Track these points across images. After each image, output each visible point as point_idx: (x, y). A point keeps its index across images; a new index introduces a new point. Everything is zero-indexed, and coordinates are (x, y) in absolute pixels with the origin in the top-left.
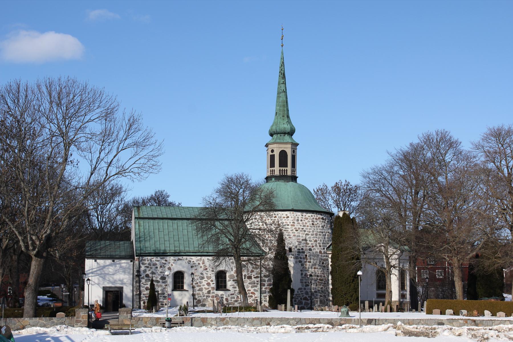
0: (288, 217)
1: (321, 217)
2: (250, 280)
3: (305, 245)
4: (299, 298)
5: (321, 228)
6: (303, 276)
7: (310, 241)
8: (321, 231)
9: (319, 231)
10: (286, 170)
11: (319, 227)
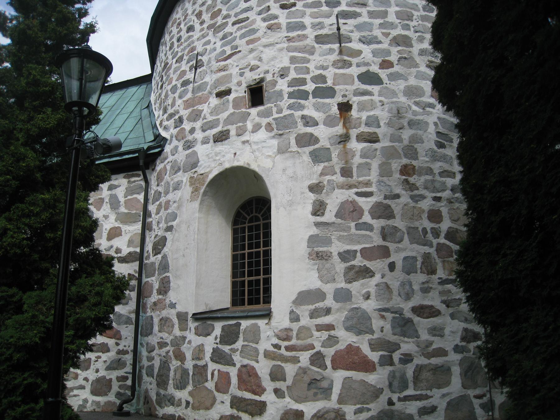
4: (305, 357)
6: (329, 216)
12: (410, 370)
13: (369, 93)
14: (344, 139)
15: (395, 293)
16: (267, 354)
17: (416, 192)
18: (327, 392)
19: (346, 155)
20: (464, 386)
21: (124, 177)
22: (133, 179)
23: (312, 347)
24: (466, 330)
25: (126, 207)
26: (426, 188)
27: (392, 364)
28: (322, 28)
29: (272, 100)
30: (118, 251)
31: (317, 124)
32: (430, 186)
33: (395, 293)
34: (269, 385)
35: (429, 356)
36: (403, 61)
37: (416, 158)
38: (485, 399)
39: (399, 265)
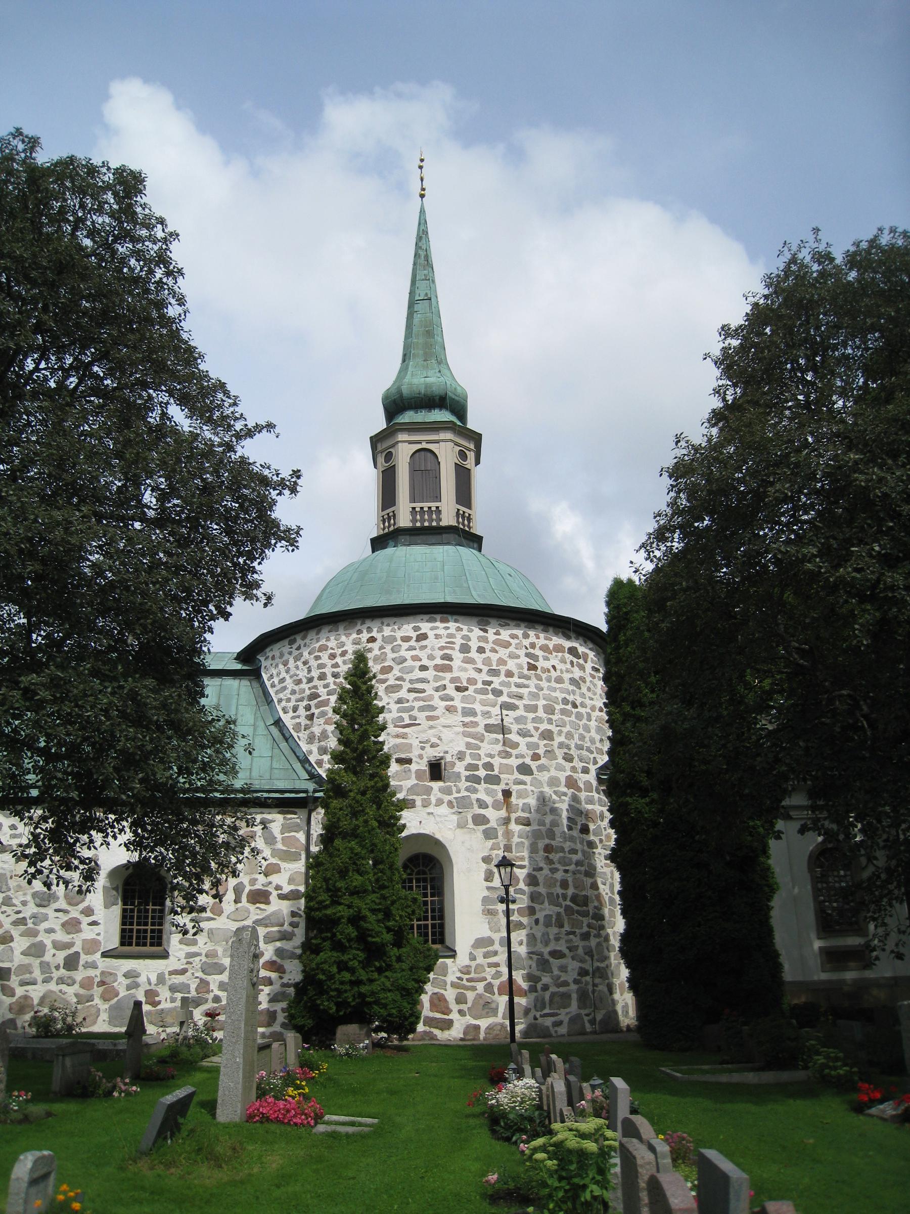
0: (423, 637)
1: (568, 644)
2: (262, 906)
3: (499, 747)
4: (480, 986)
5: (571, 688)
7: (523, 734)
8: (571, 698)
9: (560, 695)
11: (559, 680)
12: (547, 995)
13: (524, 783)
14: (507, 821)
15: (539, 941)
16: (453, 985)
17: (553, 866)
18: (495, 1012)
19: (508, 834)
20: (579, 1008)
21: (279, 813)
22: (289, 816)
23: (485, 979)
24: (581, 968)
25: (283, 844)
26: (559, 863)
27: (536, 991)
28: (490, 717)
29: (452, 780)
30: (278, 888)
31: (487, 807)
32: (564, 863)
33: (539, 941)
34: (454, 1007)
35: (559, 986)
36: (548, 755)
37: (554, 839)
38: (591, 1017)
39: (542, 920)
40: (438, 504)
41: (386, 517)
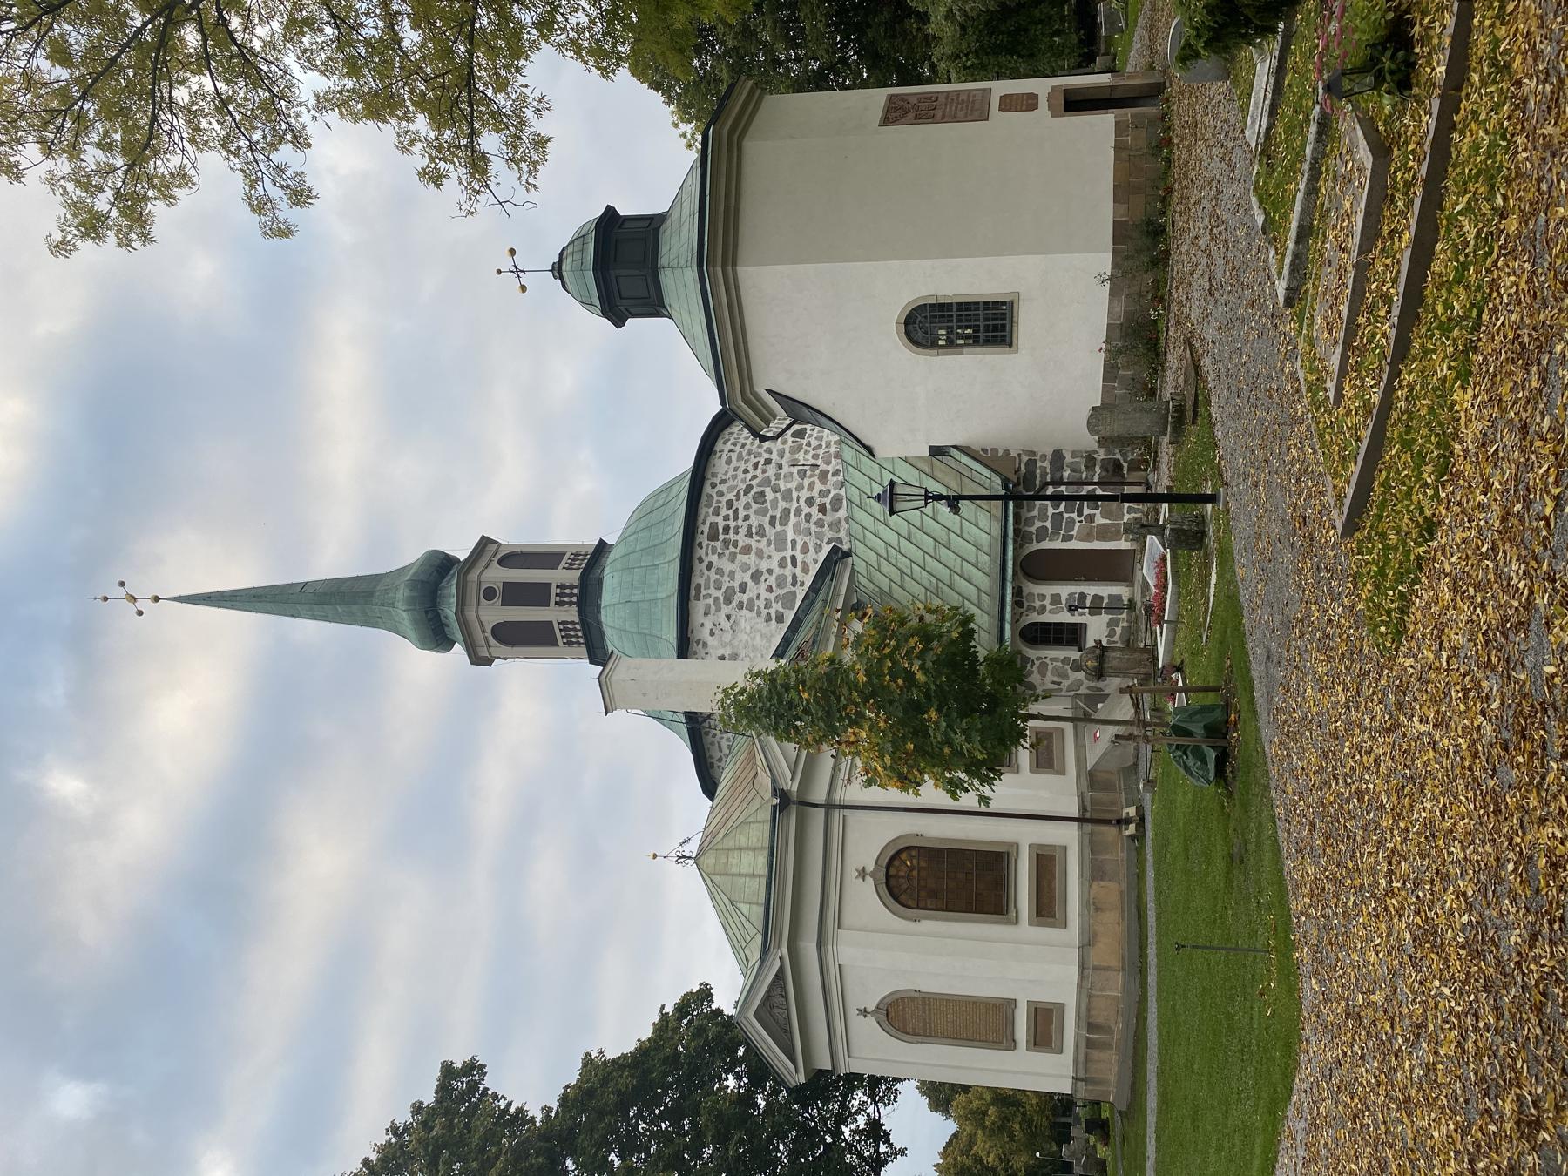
10: (559, 591)
40: (554, 587)
41: (565, 640)
